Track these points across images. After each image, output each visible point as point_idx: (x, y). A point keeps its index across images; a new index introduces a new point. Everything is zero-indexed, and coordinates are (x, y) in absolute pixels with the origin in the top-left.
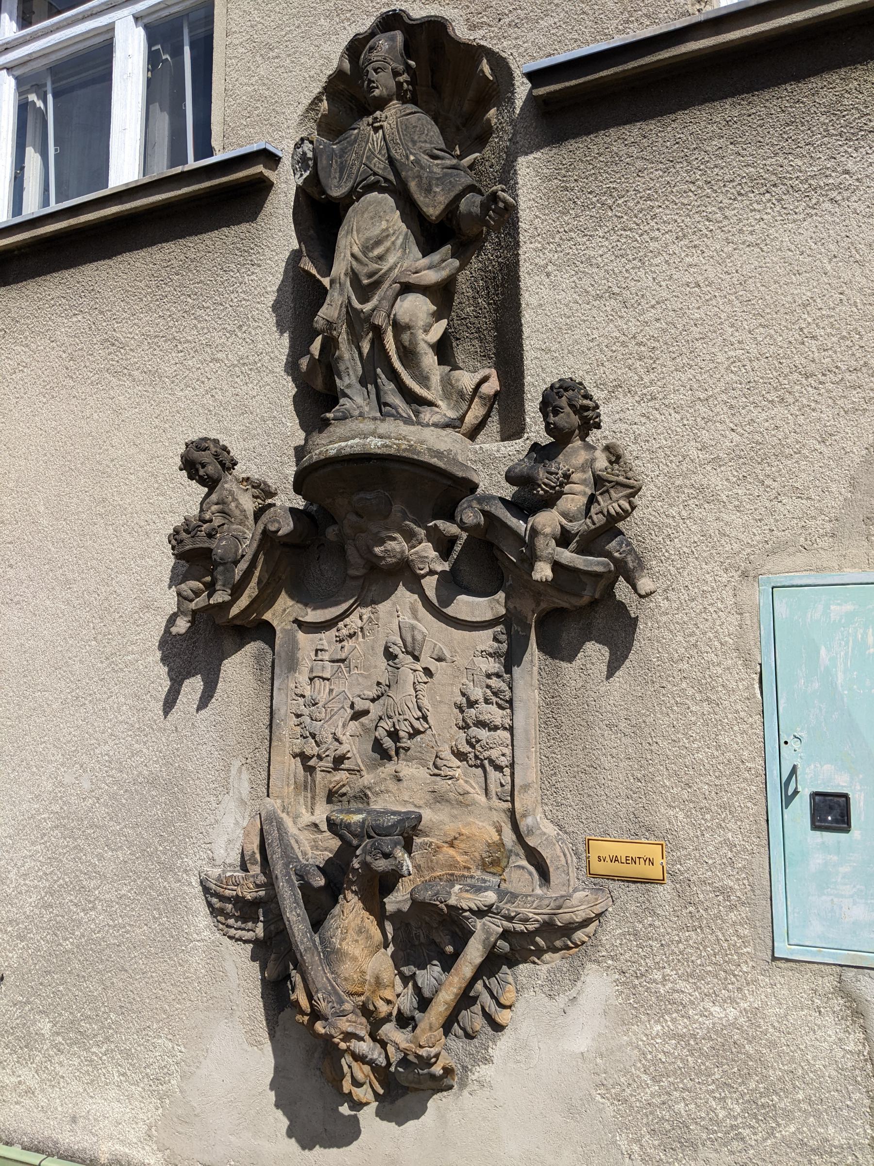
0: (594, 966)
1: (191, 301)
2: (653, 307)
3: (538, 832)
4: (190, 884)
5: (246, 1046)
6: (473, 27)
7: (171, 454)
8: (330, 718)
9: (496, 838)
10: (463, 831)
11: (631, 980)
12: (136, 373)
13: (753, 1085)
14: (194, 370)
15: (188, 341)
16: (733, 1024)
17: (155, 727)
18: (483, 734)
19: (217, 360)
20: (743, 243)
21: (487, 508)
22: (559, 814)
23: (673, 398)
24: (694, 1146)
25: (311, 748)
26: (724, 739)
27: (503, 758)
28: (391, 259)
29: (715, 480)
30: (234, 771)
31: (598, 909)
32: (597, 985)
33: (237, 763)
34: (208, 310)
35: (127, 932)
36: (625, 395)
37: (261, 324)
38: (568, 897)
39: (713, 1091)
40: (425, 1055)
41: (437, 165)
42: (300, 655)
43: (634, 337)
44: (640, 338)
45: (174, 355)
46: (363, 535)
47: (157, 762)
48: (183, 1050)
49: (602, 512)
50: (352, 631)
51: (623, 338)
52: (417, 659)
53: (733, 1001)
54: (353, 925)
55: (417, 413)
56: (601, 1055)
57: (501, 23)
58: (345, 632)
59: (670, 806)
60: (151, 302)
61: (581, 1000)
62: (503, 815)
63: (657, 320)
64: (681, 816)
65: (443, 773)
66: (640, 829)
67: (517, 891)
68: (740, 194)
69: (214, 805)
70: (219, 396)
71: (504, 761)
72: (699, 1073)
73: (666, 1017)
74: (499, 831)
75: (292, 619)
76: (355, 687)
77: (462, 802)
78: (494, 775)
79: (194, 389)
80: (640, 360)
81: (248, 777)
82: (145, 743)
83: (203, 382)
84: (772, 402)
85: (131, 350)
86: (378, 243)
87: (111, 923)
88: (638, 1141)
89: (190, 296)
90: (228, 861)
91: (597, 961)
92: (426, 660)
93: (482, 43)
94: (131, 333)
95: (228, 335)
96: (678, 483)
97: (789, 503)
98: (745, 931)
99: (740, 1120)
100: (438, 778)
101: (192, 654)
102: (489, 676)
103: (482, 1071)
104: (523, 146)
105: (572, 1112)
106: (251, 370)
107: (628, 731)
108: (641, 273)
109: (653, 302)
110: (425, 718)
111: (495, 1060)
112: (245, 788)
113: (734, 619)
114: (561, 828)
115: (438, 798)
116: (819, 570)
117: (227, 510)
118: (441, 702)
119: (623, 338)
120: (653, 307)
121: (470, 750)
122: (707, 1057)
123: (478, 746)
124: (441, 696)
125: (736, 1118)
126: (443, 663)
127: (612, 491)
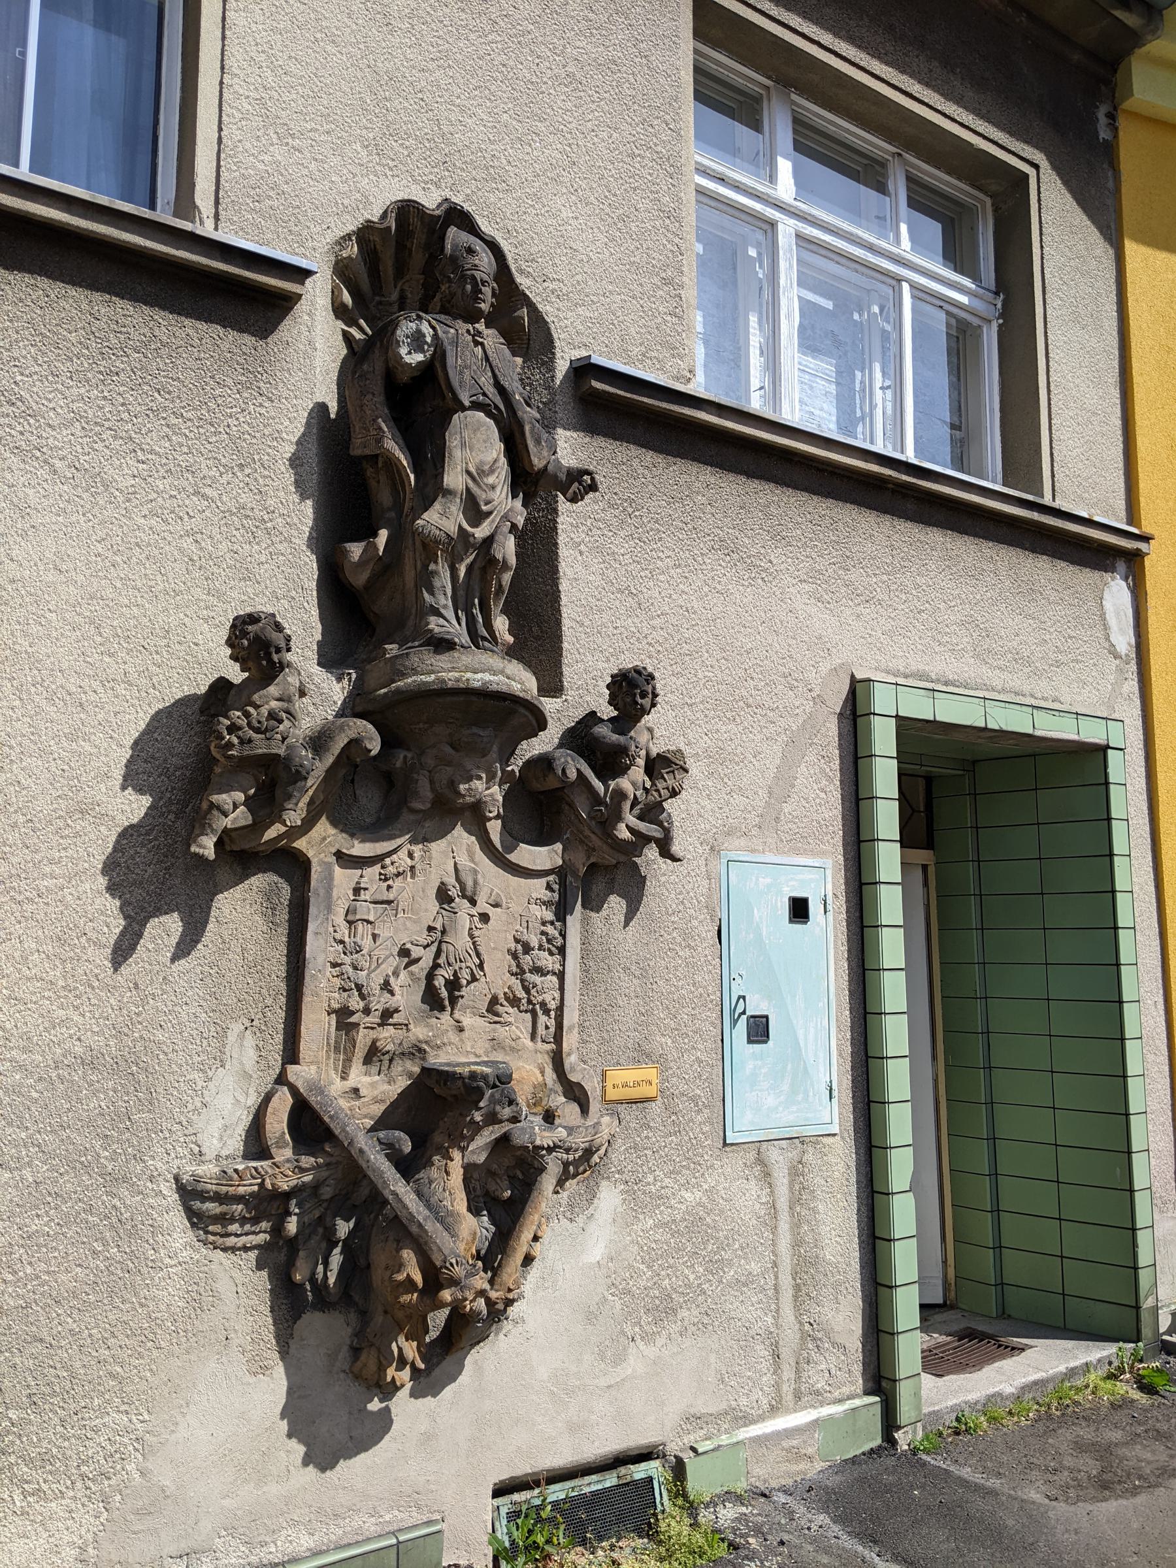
7: (126, 602)
9: (540, 1079)
12: (58, 464)
15: (152, 452)
18: (537, 979)
24: (675, 1311)
25: (356, 1003)
26: (698, 978)
30: (232, 1037)
32: (609, 1197)
33: (236, 1028)
48: (147, 1417)
50: (401, 870)
51: (638, 635)
52: (473, 902)
57: (546, 284)
58: (391, 870)
62: (546, 1056)
64: (669, 1041)
66: (642, 1055)
69: (200, 1083)
70: (207, 544)
74: (543, 1073)
75: (334, 850)
83: (181, 518)
85: (50, 426)
90: (224, 1153)
91: (608, 1178)
92: (482, 906)
94: (50, 401)
95: (221, 469)
97: (738, 799)
98: (706, 1129)
100: (498, 1026)
102: (544, 923)
105: (591, 1317)
107: (637, 973)
112: (251, 1055)
113: (706, 883)
116: (753, 851)
117: (293, 711)
124: (495, 942)
126: (498, 910)
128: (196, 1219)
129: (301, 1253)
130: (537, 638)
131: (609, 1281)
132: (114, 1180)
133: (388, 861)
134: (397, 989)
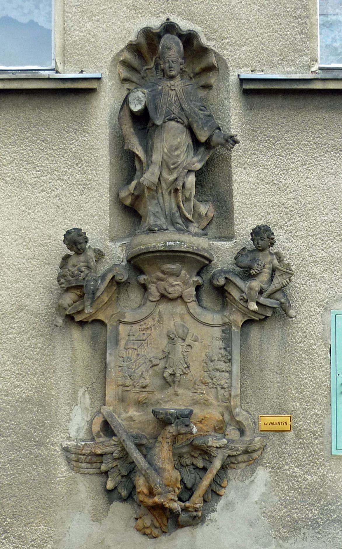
0: (261, 467)
1: (44, 144)
2: (291, 192)
3: (241, 414)
4: (55, 450)
5: (92, 523)
6: (208, 39)
7: (34, 227)
8: (139, 368)
9: (221, 418)
10: (207, 416)
11: (276, 470)
12: (8, 179)
13: (322, 503)
14: (48, 183)
15: (42, 166)
16: (315, 482)
17: (29, 373)
18: (217, 374)
19: (63, 180)
20: (329, 172)
21: (228, 277)
22: (248, 407)
23: (299, 233)
24: (300, 529)
25: (128, 382)
26: (316, 374)
27: (226, 384)
28: (183, 157)
29: (316, 270)
30: (80, 394)
31: (264, 444)
32: (262, 474)
33: (81, 391)
34: (56, 151)
35: (16, 477)
36: (279, 229)
37: (90, 165)
38: (253, 440)
39: (307, 508)
40: (198, 507)
41: (202, 114)
42: (120, 337)
43: (283, 204)
44: (286, 205)
45: (34, 172)
46: (163, 282)
47: (31, 391)
48: (54, 530)
49: (279, 283)
50: (149, 326)
51: (278, 204)
52: (184, 340)
53: (315, 473)
54: (166, 457)
55: (187, 227)
56: (264, 502)
57: (223, 41)
59: (294, 401)
60: (17, 140)
61: (256, 480)
62: (224, 408)
63: (294, 199)
64: (298, 404)
65: (198, 392)
66: (281, 411)
67: (234, 439)
68: (327, 151)
69: (69, 411)
71: (226, 386)
72: (302, 502)
73: (290, 483)
74: (223, 416)
75: (116, 320)
76: (151, 352)
77: (206, 404)
78: (221, 391)
79: (48, 193)
80: (286, 214)
81: (89, 397)
82: (23, 381)
83: (53, 190)
84: (338, 240)
85: (4, 165)
86: (176, 149)
87: (5, 474)
88: (278, 531)
89: (43, 141)
90: (79, 438)
91: (262, 465)
92: (188, 341)
93: (213, 48)
94: (4, 156)
95: (69, 167)
96: (300, 269)
98: (320, 447)
99: (317, 516)
100: (196, 394)
101: (51, 335)
102: (220, 349)
103: (212, 515)
104: (233, 105)
106: (84, 188)
107: (278, 372)
108: (287, 177)
109: (292, 191)
110: (188, 367)
111: (217, 510)
112: (88, 401)
113: (321, 327)
114: (248, 413)
115: (196, 403)
117: (90, 266)
118: (195, 360)
119: (278, 204)
120: (291, 192)
121: (211, 381)
122: (305, 495)
123: (214, 379)
124: (195, 357)
125: (315, 516)
126: (197, 343)
127: (284, 275)
128: (69, 461)
129: (109, 479)
130: (225, 212)
131: (262, 511)
132: (39, 444)
133: (142, 323)
134: (147, 377)
